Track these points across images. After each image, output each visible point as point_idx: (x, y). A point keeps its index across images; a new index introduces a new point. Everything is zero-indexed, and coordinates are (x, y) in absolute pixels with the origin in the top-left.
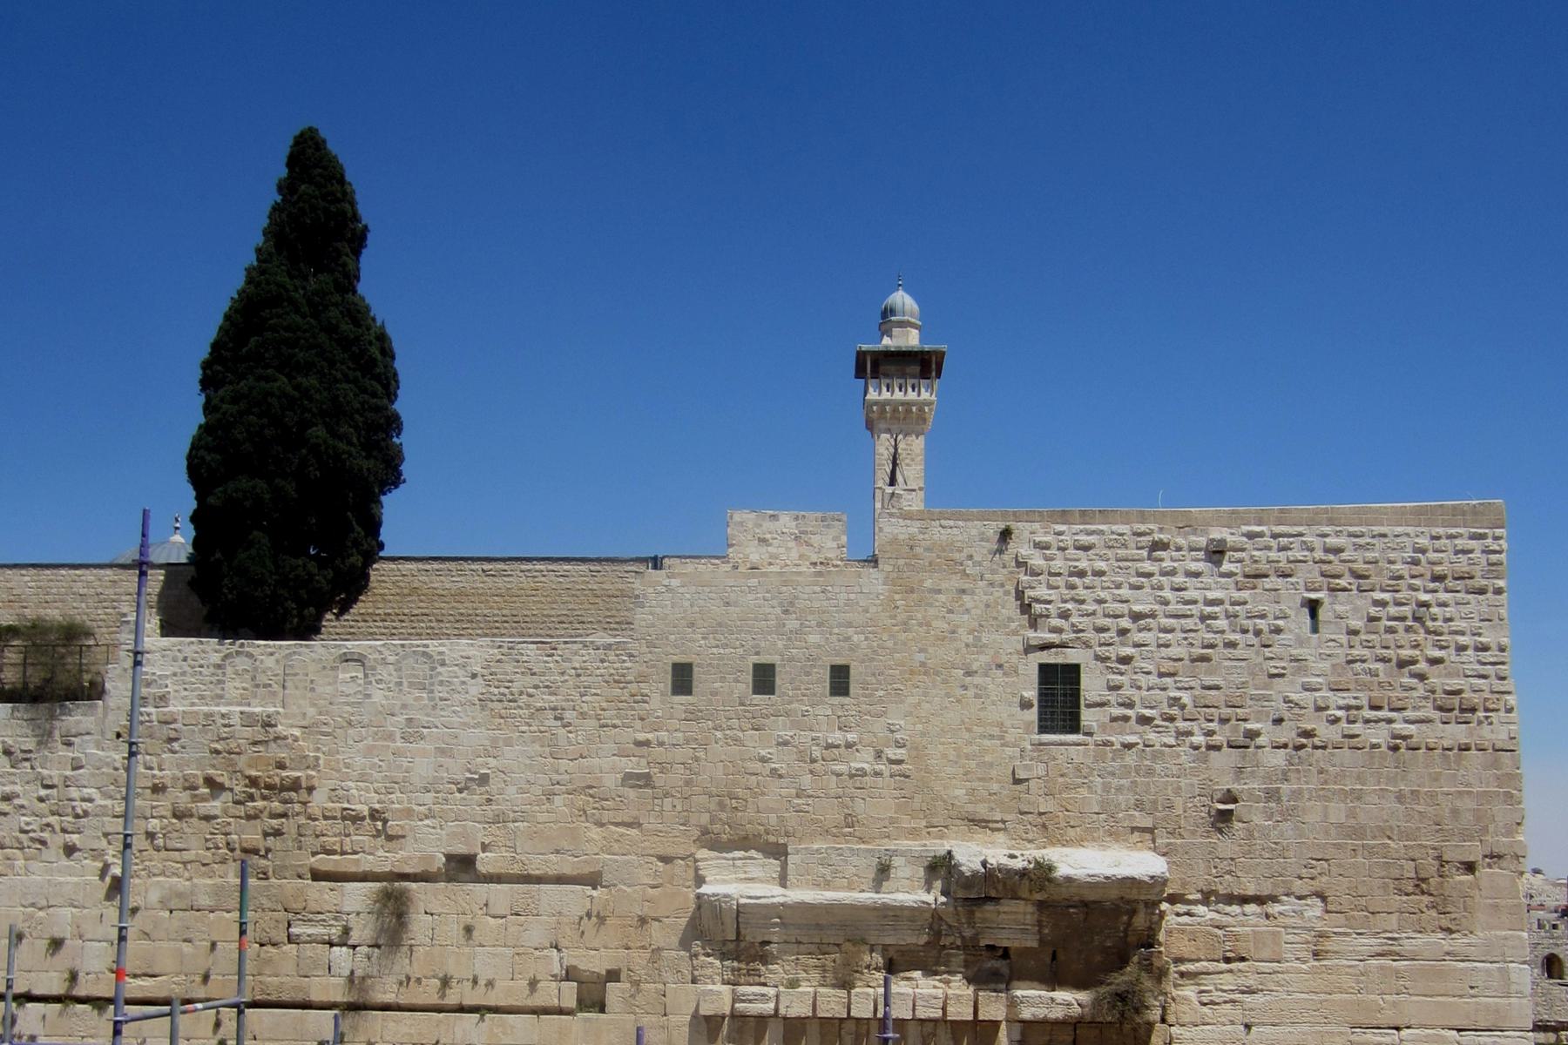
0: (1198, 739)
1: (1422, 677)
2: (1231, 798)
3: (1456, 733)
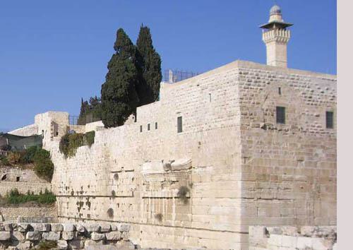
0: (196, 130)
1: (225, 109)
2: (200, 143)
3: (230, 122)
